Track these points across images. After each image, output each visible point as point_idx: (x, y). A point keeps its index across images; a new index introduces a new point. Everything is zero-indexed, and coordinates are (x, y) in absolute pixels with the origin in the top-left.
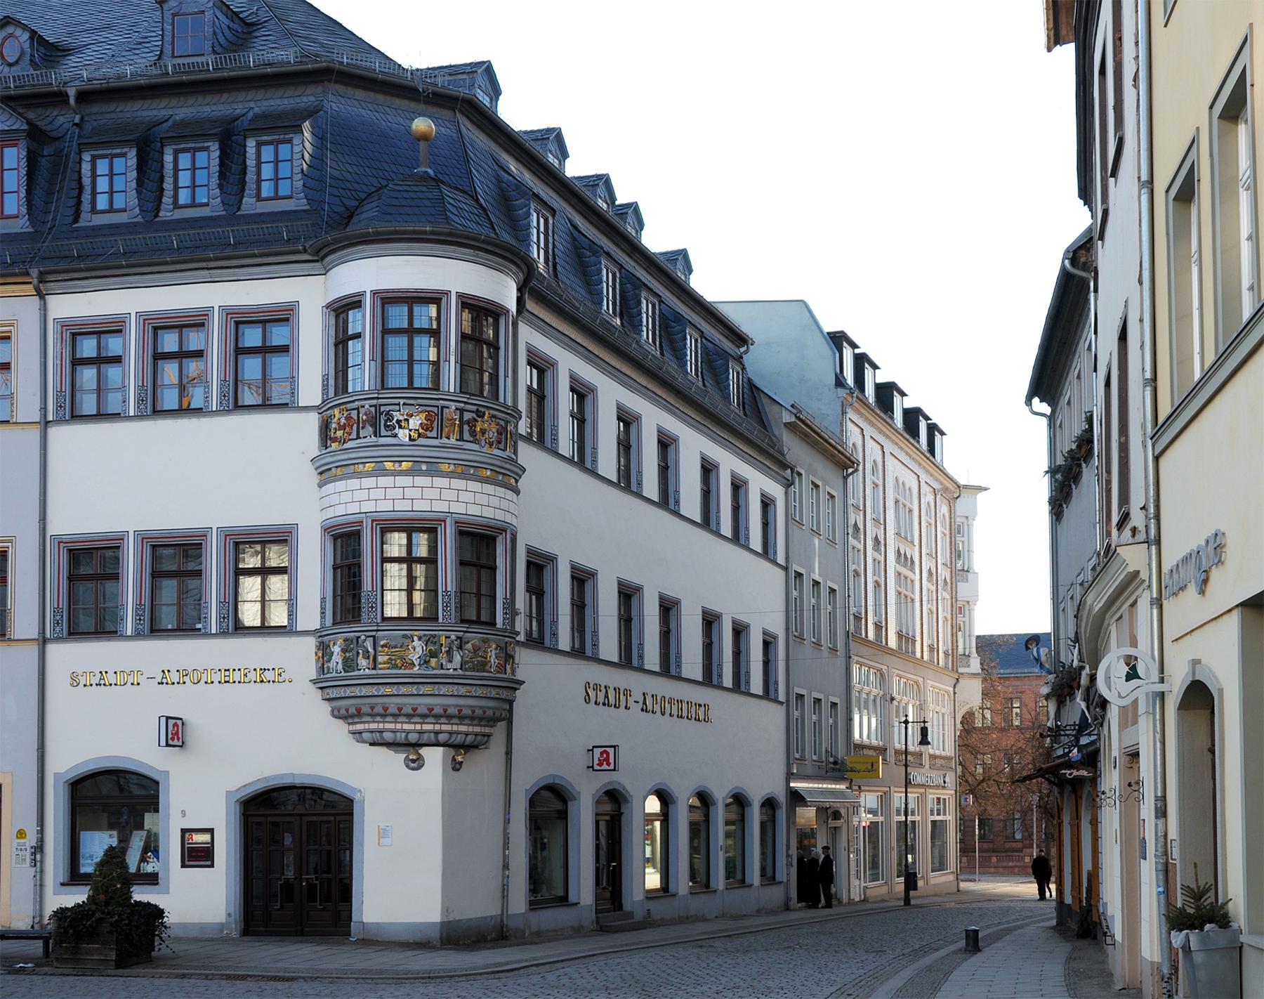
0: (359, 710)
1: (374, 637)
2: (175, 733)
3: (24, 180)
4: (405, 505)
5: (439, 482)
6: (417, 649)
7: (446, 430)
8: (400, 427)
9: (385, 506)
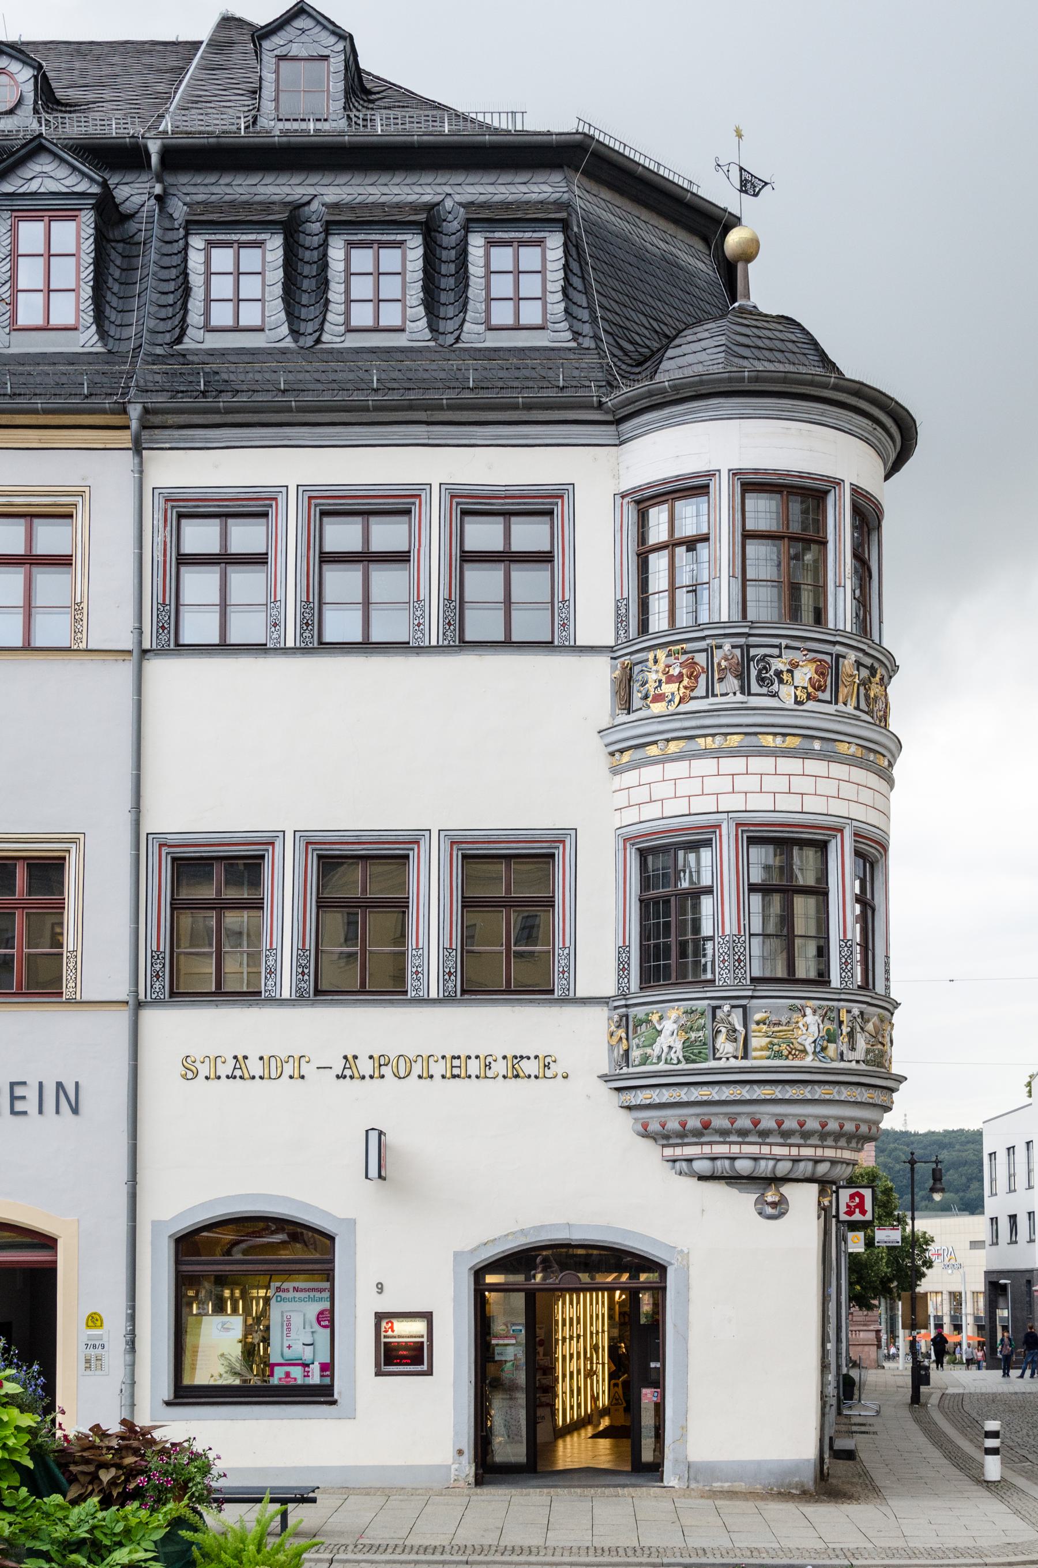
0: (706, 1125)
1: (744, 1007)
2: (379, 1159)
3: (88, 274)
4: (790, 803)
5: (839, 770)
6: (809, 1027)
8: (781, 681)
9: (762, 802)
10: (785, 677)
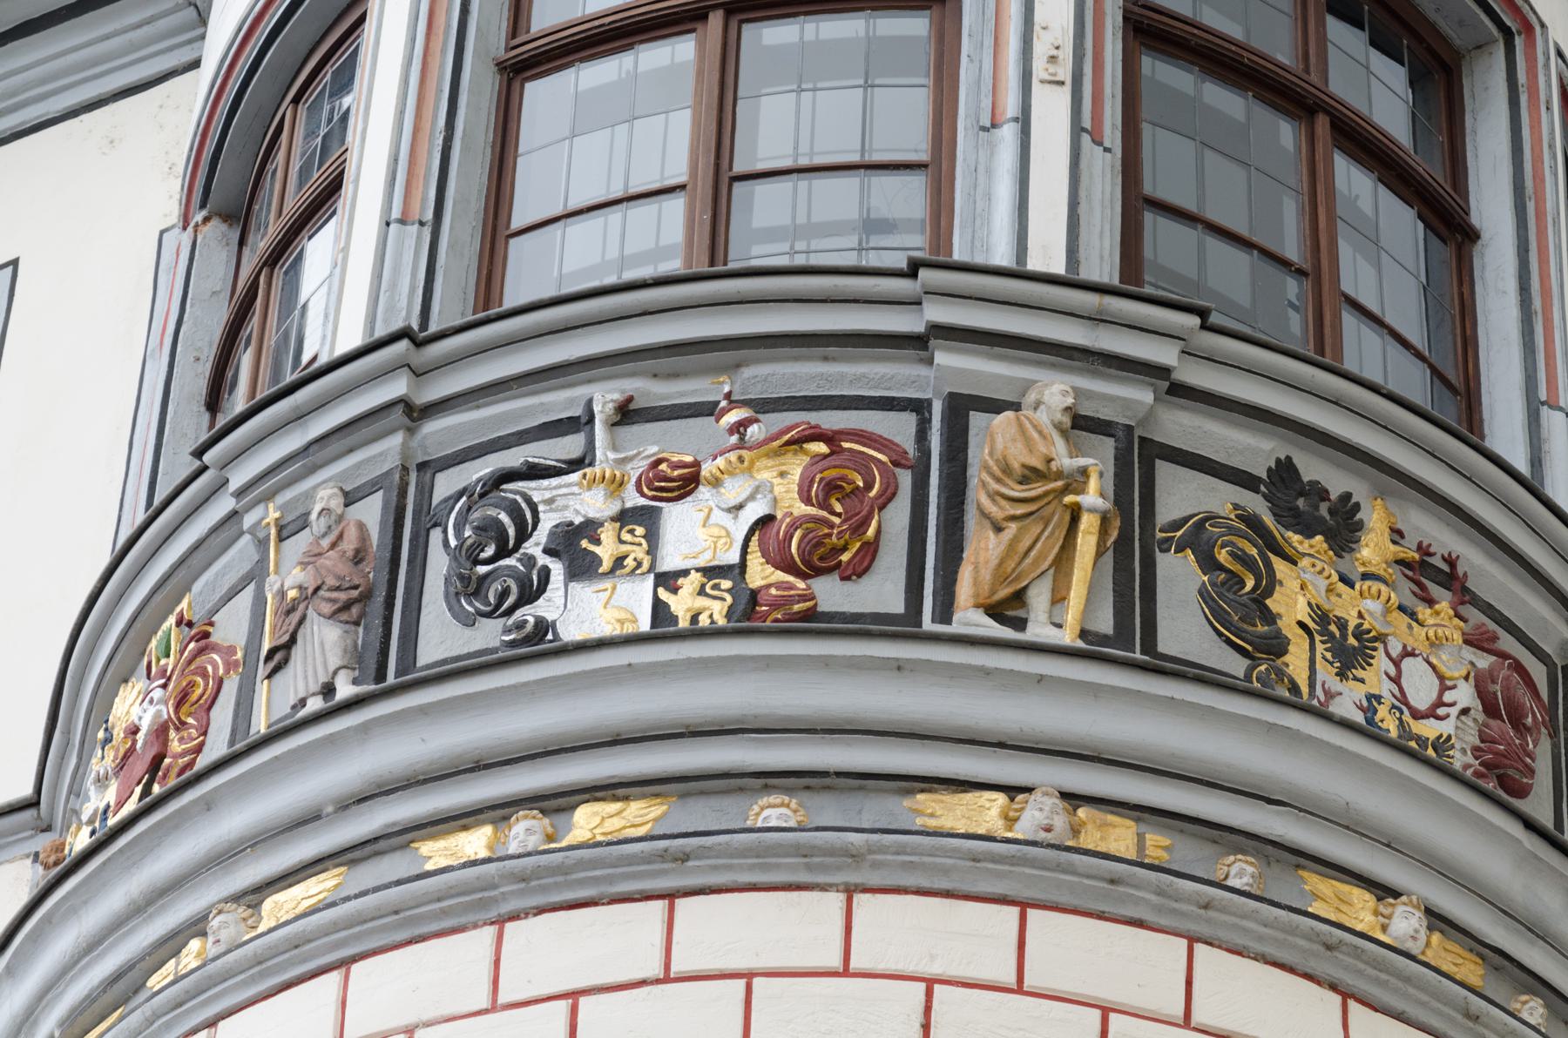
7: (984, 551)
8: (582, 568)
10: (606, 551)
